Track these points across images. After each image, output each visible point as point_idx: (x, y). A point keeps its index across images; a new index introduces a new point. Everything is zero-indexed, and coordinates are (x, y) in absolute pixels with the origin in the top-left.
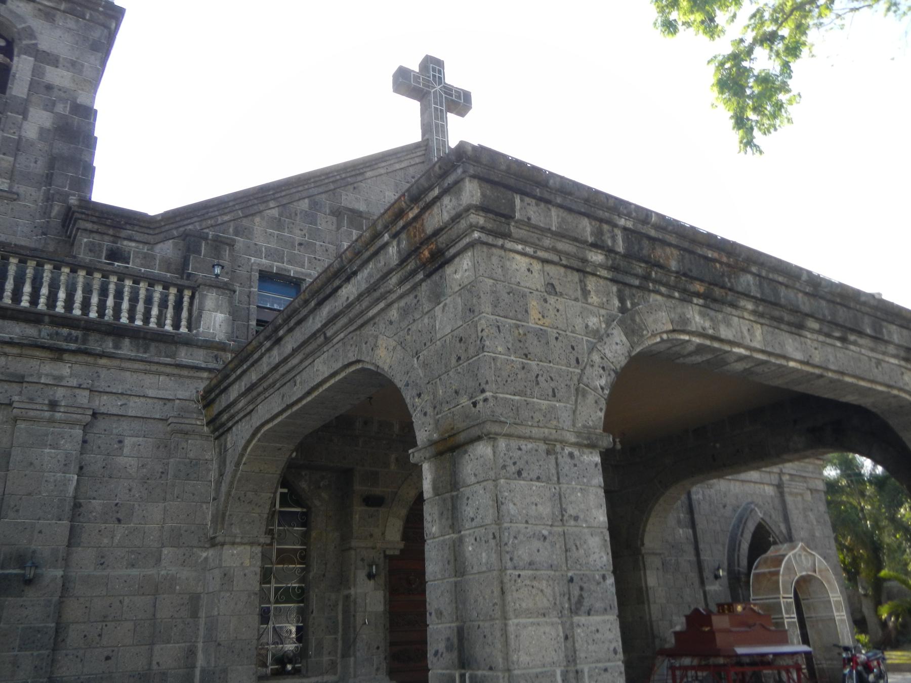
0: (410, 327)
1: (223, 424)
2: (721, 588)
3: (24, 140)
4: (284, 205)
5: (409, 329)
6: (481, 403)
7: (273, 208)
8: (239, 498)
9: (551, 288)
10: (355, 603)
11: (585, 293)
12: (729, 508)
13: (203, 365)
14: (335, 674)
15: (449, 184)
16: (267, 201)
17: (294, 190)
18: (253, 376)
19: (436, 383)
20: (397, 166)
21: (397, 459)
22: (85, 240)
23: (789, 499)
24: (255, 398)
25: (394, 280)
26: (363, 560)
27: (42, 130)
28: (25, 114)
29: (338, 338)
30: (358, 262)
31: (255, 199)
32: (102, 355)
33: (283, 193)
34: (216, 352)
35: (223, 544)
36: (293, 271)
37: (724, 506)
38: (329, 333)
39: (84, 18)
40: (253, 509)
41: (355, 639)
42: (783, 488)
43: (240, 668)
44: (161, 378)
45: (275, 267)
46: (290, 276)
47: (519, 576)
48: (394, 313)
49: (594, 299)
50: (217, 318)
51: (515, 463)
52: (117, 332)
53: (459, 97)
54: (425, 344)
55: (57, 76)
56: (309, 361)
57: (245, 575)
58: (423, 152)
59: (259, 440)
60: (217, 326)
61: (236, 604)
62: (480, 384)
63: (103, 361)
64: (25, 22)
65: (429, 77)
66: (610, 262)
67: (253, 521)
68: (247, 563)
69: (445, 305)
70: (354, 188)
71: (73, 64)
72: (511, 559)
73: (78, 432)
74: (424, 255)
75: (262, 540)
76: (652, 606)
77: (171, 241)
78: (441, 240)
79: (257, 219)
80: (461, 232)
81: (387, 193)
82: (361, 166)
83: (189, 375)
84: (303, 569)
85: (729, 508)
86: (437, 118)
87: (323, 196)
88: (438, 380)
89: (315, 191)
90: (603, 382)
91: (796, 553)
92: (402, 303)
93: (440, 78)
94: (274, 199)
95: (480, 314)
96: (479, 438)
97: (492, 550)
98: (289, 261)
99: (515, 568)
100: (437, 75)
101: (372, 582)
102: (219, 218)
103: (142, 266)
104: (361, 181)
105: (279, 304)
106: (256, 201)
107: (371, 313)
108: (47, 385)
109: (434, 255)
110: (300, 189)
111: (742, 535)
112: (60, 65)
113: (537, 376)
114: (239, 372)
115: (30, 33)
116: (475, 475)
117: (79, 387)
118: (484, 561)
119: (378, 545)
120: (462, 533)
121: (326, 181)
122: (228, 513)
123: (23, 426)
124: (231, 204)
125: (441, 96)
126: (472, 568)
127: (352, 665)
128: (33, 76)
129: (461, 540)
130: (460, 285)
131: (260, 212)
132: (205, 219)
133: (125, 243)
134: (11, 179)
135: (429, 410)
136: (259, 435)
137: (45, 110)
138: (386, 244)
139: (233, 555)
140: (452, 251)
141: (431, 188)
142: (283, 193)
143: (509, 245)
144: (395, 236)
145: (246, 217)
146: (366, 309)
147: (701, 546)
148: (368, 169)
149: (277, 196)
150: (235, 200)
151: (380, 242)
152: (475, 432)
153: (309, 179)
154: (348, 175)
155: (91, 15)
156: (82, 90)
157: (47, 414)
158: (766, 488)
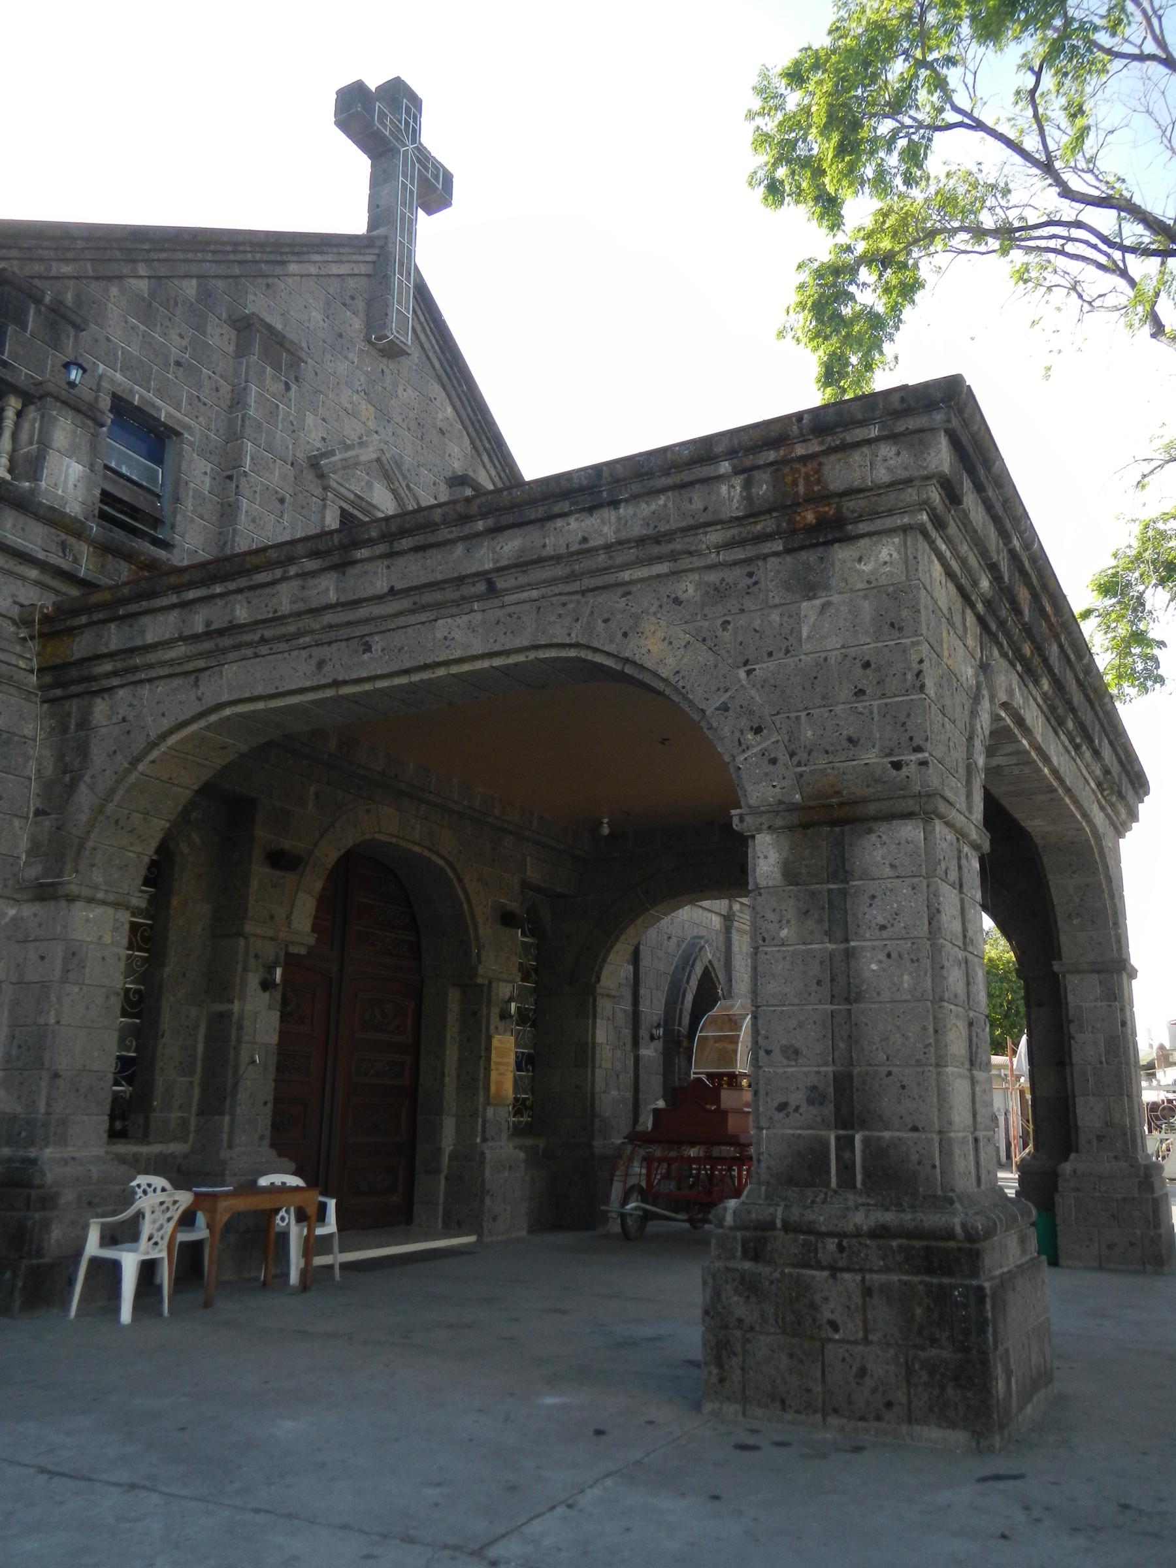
0: (728, 618)
1: (95, 678)
2: (654, 1054)
4: (159, 278)
5: (728, 622)
6: (913, 766)
7: (141, 277)
8: (117, 822)
10: (240, 1028)
12: (674, 940)
13: (41, 555)
14: (186, 1142)
15: (907, 429)
16: (134, 261)
17: (180, 256)
18: (242, 614)
19: (798, 718)
21: (316, 794)
23: (735, 937)
24: (224, 651)
25: (715, 537)
26: (257, 956)
29: (524, 596)
30: (635, 488)
31: (120, 249)
33: (163, 255)
34: (63, 536)
35: (71, 899)
36: (165, 412)
37: (669, 938)
38: (500, 584)
40: (132, 844)
41: (235, 1086)
42: (732, 921)
43: (86, 1118)
45: (138, 395)
46: (158, 420)
48: (688, 588)
50: (70, 471)
53: (436, 177)
54: (770, 654)
56: (423, 617)
57: (104, 958)
58: (374, 258)
59: (208, 727)
60: (70, 485)
61: (87, 1008)
62: (911, 739)
65: (400, 122)
67: (127, 866)
68: (107, 939)
69: (829, 604)
70: (268, 286)
74: (804, 518)
75: (135, 902)
76: (597, 1071)
78: (851, 504)
79: (114, 291)
80: (901, 504)
81: (314, 314)
82: (287, 249)
83: (6, 567)
84: (145, 959)
85: (674, 940)
86: (404, 204)
87: (220, 284)
88: (803, 714)
89: (213, 269)
92: (712, 577)
93: (414, 130)
94: (148, 261)
95: (917, 635)
96: (909, 815)
97: (926, 973)
98: (158, 390)
100: (412, 123)
101: (267, 995)
102: (54, 264)
104: (278, 277)
105: (129, 467)
106: (118, 254)
107: (626, 575)
109: (823, 524)
110: (190, 256)
111: (688, 982)
114: (191, 595)
116: (892, 866)
118: (906, 985)
119: (282, 935)
120: (853, 944)
121: (231, 257)
122: (90, 844)
124: (80, 244)
126: (878, 994)
127: (226, 1128)
129: (849, 954)
130: (869, 582)
131: (120, 277)
132: (31, 259)
135: (783, 757)
136: (213, 718)
138: (719, 478)
139: (88, 920)
140: (863, 527)
141: (864, 423)
142: (163, 255)
144: (737, 472)
145: (96, 278)
146: (618, 566)
147: (642, 992)
148: (295, 258)
149: (154, 255)
150: (87, 239)
151: (706, 471)
152: (910, 805)
153: (208, 243)
154: (265, 257)
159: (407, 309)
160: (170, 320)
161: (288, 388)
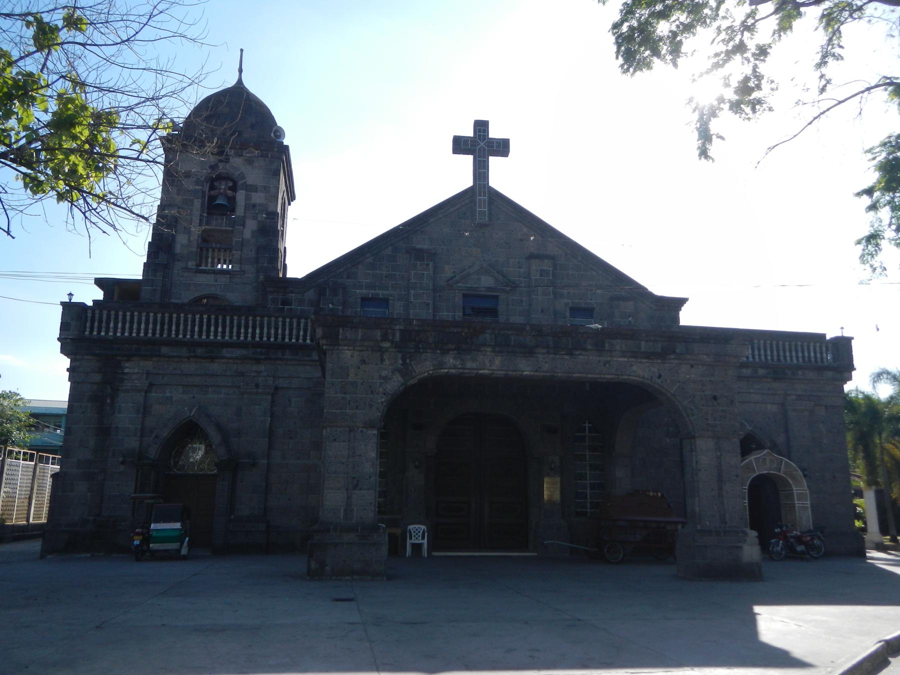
3: (245, 240)
9: (363, 362)
11: (382, 360)
20: (452, 210)
22: (271, 297)
27: (253, 232)
28: (244, 225)
32: (277, 359)
36: (381, 293)
39: (268, 158)
44: (307, 367)
45: (370, 293)
47: (330, 476)
49: (387, 362)
51: (333, 436)
52: (283, 347)
55: (258, 198)
63: (279, 362)
64: (238, 171)
66: (394, 345)
70: (422, 232)
71: (265, 187)
72: (327, 470)
73: (269, 397)
77: (313, 289)
79: (360, 266)
90: (383, 400)
91: (760, 457)
99: (328, 473)
103: (298, 306)
108: (254, 376)
112: (259, 191)
113: (349, 401)
115: (242, 176)
117: (268, 376)
123: (245, 396)
125: (484, 149)
128: (246, 200)
133: (290, 295)
134: (241, 264)
137: (254, 219)
143: (341, 348)
155: (271, 154)
156: (271, 202)
157: (255, 390)
158: (769, 406)
159: (485, 207)
160: (381, 264)
161: (427, 265)
